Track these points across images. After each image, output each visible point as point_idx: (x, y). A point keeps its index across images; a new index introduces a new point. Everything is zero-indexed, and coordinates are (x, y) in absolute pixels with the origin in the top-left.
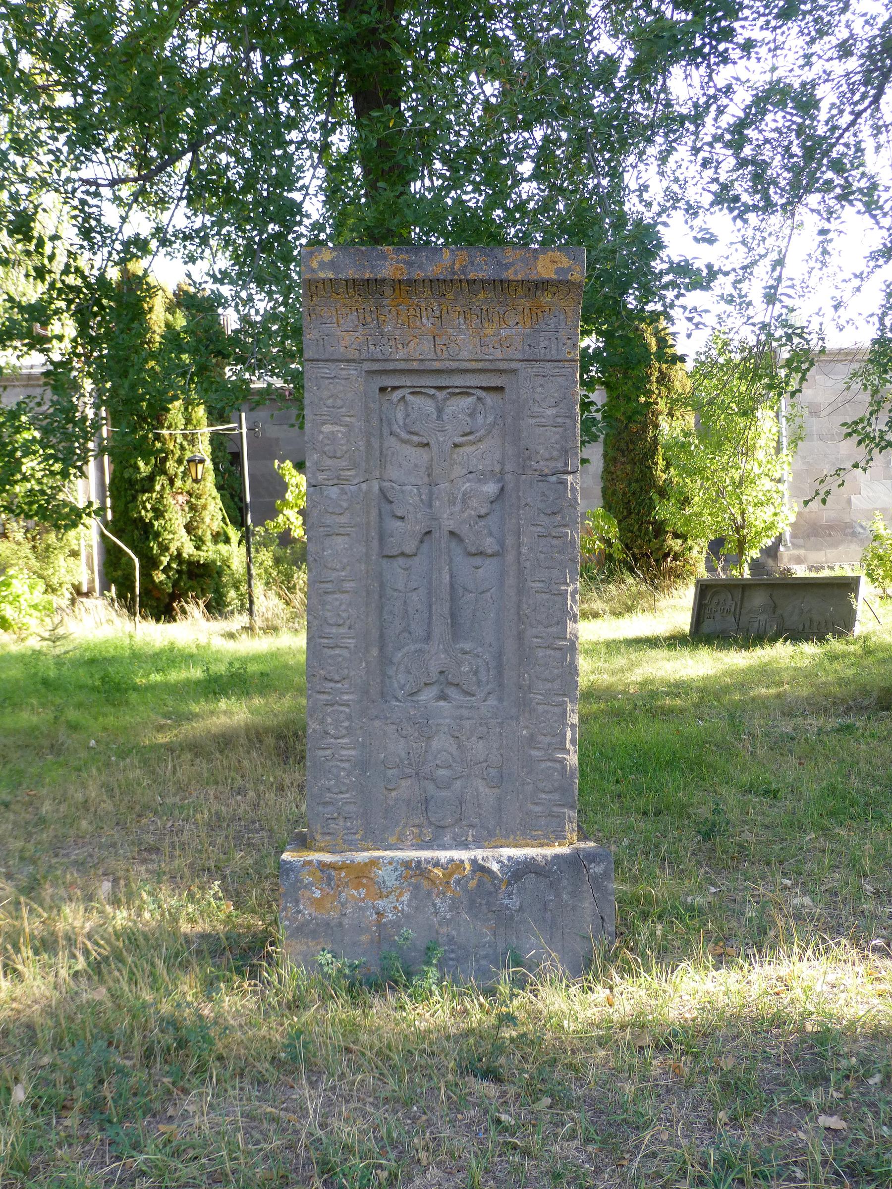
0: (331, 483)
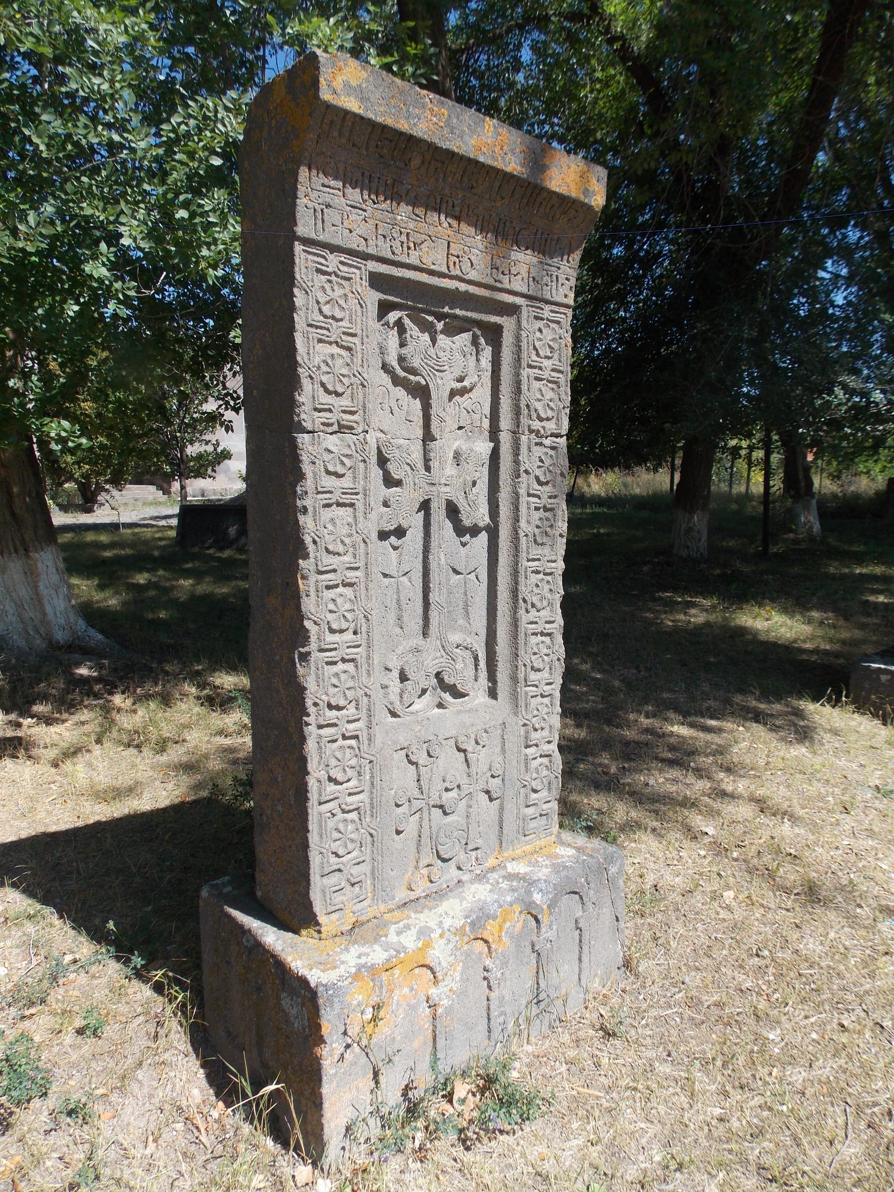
0: (330, 430)
